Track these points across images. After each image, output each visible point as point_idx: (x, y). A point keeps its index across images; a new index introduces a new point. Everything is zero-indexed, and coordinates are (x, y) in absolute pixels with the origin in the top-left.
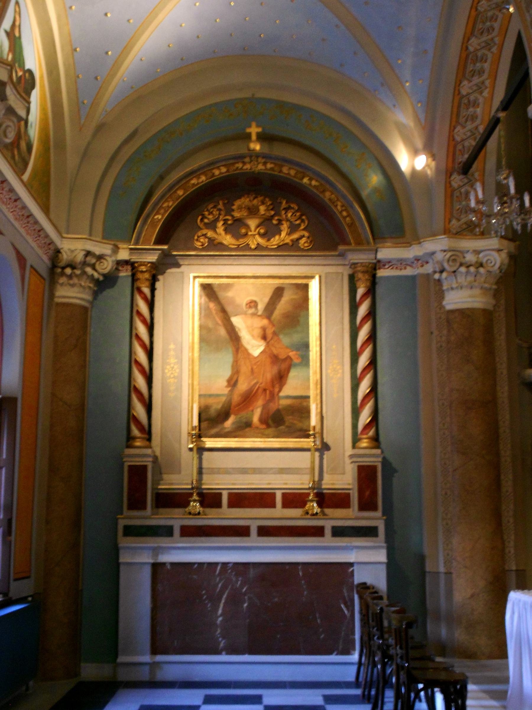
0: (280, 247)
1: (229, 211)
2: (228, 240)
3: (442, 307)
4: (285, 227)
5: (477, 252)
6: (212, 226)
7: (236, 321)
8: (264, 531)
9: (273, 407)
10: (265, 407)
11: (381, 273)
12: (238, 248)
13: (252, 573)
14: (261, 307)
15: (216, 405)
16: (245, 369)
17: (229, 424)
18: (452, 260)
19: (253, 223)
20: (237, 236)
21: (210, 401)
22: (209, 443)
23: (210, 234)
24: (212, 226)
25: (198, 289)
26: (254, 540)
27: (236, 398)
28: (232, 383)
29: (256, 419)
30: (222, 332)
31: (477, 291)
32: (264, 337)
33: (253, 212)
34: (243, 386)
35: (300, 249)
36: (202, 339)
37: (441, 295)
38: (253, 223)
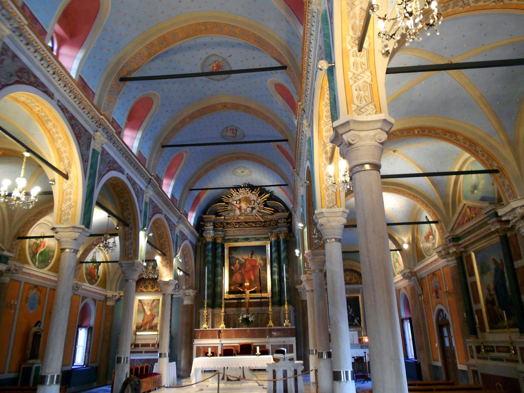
0: (155, 291)
1: (145, 284)
2: (144, 290)
3: (183, 304)
4: (156, 287)
5: (189, 293)
6: (141, 287)
7: (145, 307)
8: (146, 352)
9: (151, 325)
10: (149, 326)
11: (174, 296)
12: (147, 292)
13: (142, 361)
14: (150, 304)
15: (139, 325)
16: (146, 317)
17: (142, 329)
18: (184, 295)
19: (150, 286)
20: (146, 289)
21: (139, 324)
22: (138, 333)
23: (141, 289)
24: (141, 287)
25: (138, 301)
26: (144, 354)
27: (144, 324)
28: (143, 320)
29: (147, 328)
30: (142, 310)
31: (189, 301)
32: (150, 310)
33: (150, 283)
34: (145, 321)
35: (158, 292)
36: (138, 311)
37: (183, 302)
38: (150, 286)
